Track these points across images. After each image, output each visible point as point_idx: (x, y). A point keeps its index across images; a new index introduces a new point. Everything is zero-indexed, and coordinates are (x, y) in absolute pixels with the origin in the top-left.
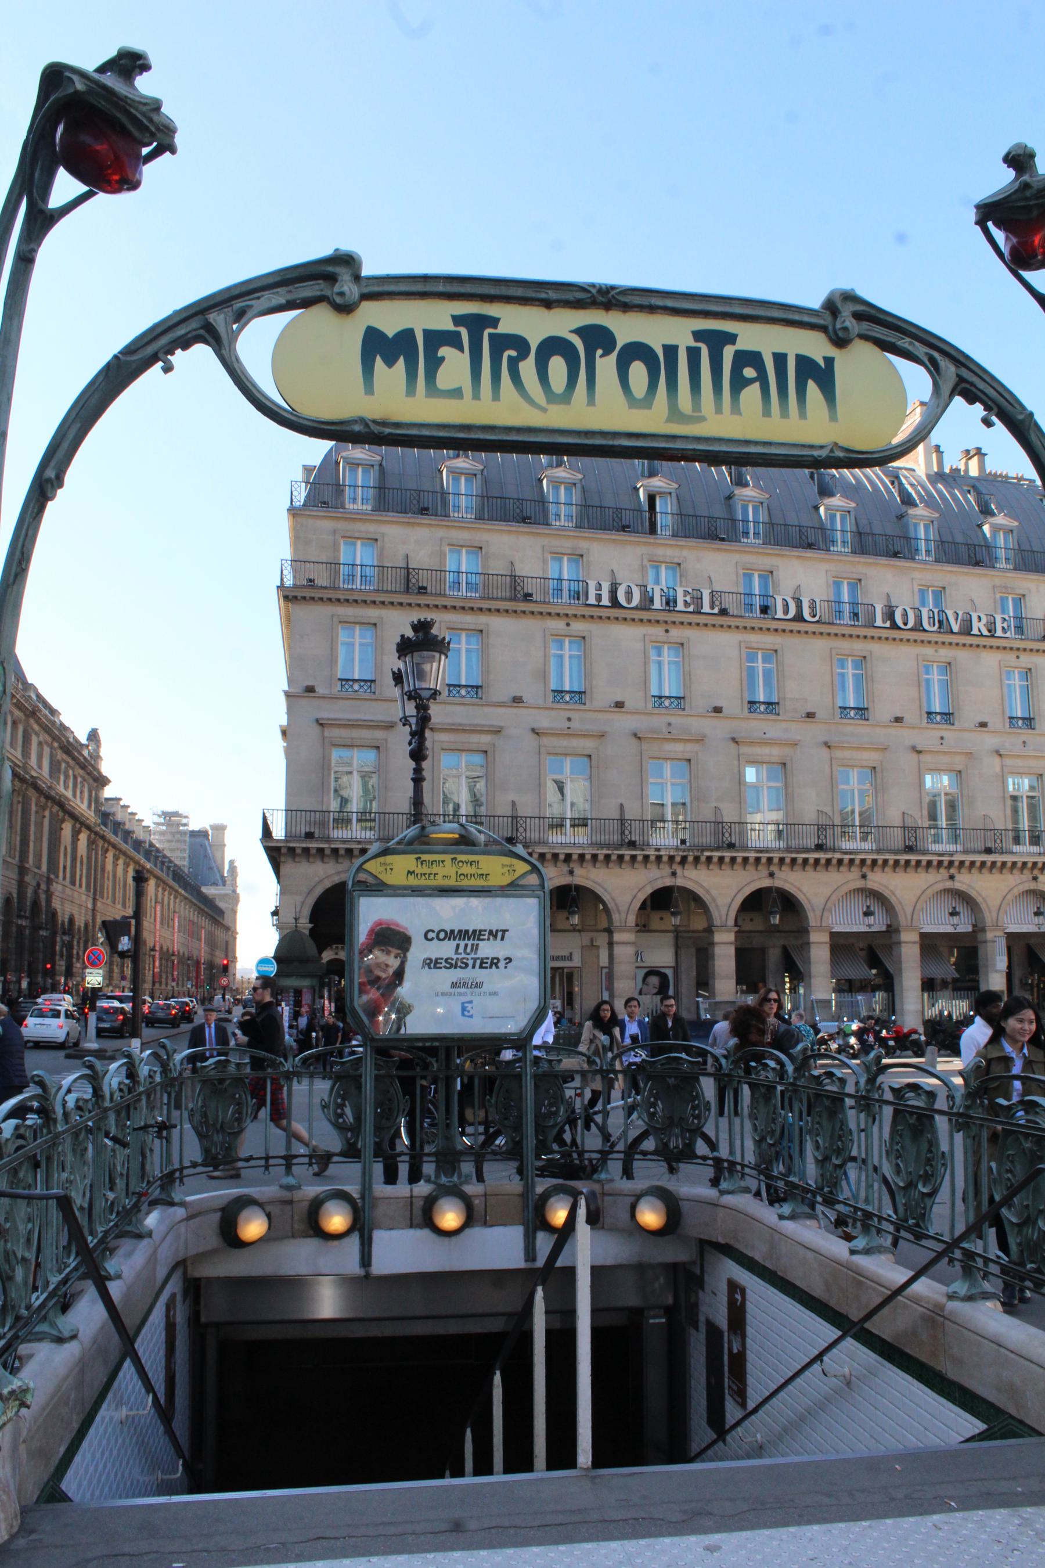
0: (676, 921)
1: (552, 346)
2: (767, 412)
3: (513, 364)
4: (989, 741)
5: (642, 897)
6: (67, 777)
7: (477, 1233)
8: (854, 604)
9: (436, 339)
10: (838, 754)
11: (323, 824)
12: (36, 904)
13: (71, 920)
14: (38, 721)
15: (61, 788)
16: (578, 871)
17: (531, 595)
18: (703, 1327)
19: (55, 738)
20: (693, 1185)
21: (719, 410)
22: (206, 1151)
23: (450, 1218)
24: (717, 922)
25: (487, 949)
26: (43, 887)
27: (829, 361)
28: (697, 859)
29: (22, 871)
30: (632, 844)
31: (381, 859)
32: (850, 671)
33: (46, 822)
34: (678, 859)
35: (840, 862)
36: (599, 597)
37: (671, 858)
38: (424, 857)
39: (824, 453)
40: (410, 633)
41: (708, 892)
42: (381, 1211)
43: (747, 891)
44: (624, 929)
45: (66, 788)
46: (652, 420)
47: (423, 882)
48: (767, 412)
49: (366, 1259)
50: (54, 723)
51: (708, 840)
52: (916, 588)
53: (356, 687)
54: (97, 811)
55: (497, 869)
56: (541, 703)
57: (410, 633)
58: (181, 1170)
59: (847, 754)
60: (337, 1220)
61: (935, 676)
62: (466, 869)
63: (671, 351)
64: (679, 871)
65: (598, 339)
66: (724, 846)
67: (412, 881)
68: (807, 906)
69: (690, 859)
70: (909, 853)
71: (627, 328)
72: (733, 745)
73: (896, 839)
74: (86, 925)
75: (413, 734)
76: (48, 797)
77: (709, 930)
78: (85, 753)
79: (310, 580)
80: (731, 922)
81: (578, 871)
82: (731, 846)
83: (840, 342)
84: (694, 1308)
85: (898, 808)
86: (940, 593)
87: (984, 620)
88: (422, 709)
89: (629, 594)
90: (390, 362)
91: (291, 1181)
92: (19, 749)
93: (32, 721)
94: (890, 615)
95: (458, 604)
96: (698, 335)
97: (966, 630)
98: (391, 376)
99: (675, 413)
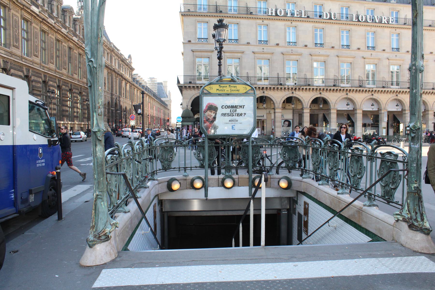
0: (293, 106)
4: (385, 55)
5: (284, 99)
6: (123, 68)
7: (236, 188)
8: (347, 14)
10: (341, 59)
11: (194, 79)
12: (116, 104)
13: (126, 108)
14: (114, 53)
15: (121, 72)
16: (266, 92)
17: (252, 13)
18: (297, 214)
20: (295, 176)
22: (163, 166)
23: (229, 184)
24: (305, 107)
25: (239, 111)
26: (118, 99)
28: (299, 89)
29: (112, 95)
30: (281, 84)
31: (209, 86)
32: (345, 34)
34: (294, 89)
35: (340, 90)
36: (272, 13)
37: (292, 88)
38: (221, 85)
40: (217, 23)
41: (302, 98)
42: (210, 182)
43: (314, 98)
44: (278, 108)
45: (123, 71)
47: (221, 92)
49: (206, 195)
50: (118, 53)
51: (302, 83)
52: (366, 9)
53: (203, 40)
54: (132, 77)
55: (242, 88)
56: (255, 44)
57: (217, 23)
58: (156, 171)
59: (343, 59)
60: (198, 184)
61: (370, 36)
62: (233, 89)
64: (294, 92)
66: (307, 85)
67: (218, 92)
68: (330, 102)
69: (297, 89)
70: (360, 88)
72: (310, 56)
73: (357, 83)
74: (130, 109)
75: (218, 52)
76: (118, 74)
77: (302, 109)
78: (128, 61)
80: (309, 106)
81: (266, 92)
82: (309, 85)
84: (295, 209)
85: (358, 74)
86: (373, 10)
87: (386, 19)
88: (221, 45)
89: (281, 12)
91: (186, 174)
92: (109, 61)
93: (112, 53)
94: (358, 18)
95: (231, 16)
97: (381, 22)
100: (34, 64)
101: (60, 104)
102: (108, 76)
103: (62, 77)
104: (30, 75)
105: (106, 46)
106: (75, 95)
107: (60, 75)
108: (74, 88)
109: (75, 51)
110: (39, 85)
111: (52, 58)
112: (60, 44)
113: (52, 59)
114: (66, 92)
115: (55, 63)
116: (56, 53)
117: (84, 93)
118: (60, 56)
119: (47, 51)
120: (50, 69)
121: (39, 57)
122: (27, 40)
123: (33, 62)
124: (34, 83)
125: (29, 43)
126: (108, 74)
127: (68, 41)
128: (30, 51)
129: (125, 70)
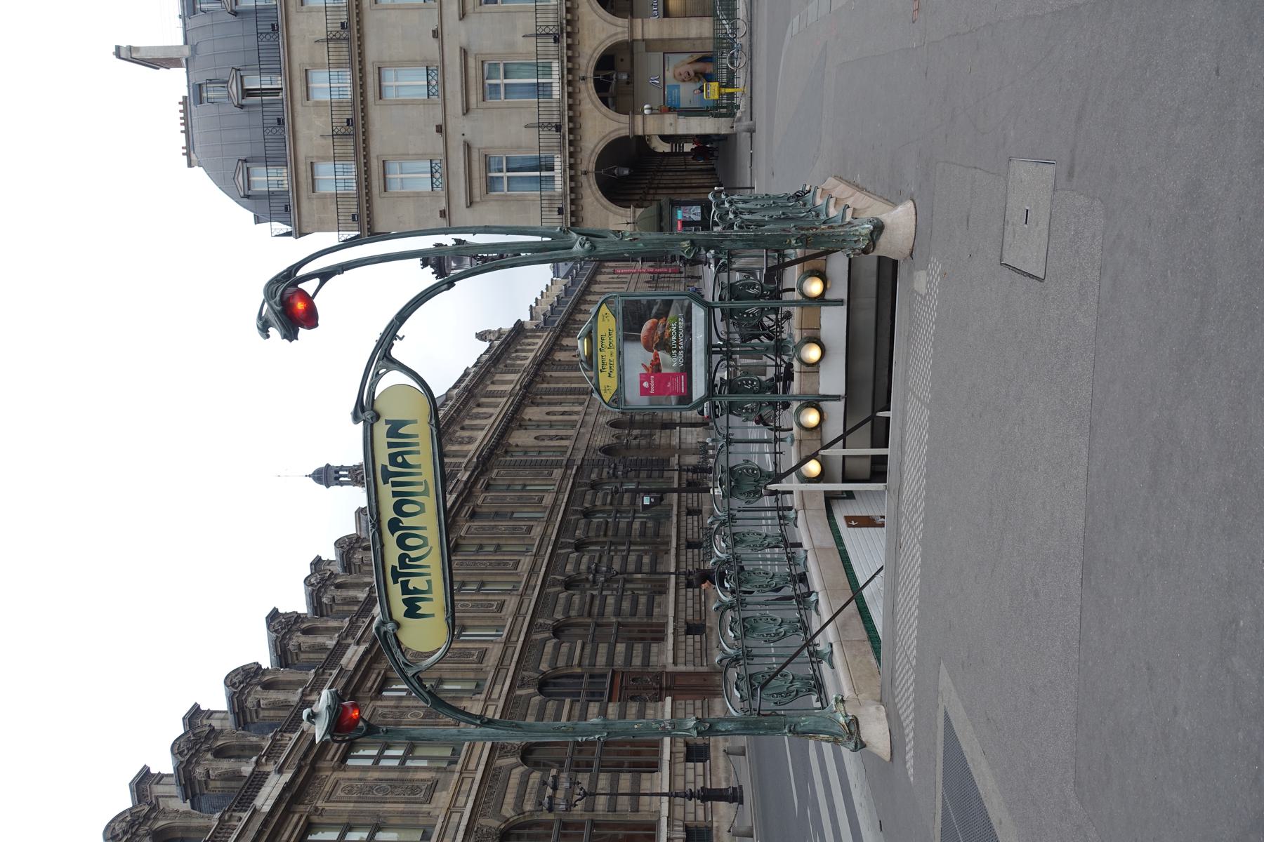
1: (401, 542)
2: (418, 452)
6: (518, 358)
7: (824, 334)
9: (405, 589)
11: (551, 199)
17: (342, 24)
19: (488, 371)
21: (420, 474)
23: (813, 353)
27: (387, 422)
33: (555, 374)
45: (526, 358)
46: (430, 502)
47: (615, 368)
48: (418, 452)
50: (476, 373)
54: (542, 330)
60: (812, 418)
62: (606, 343)
63: (395, 494)
65: (394, 525)
67: (615, 374)
71: (388, 513)
76: (536, 375)
78: (497, 343)
79: (353, 216)
83: (377, 416)
90: (419, 608)
91: (789, 440)
92: (499, 400)
95: (359, 91)
96: (386, 482)
98: (424, 607)
99: (426, 493)
100: (523, 610)
101: (624, 544)
102: (543, 404)
104: (550, 622)
105: (458, 411)
106: (598, 503)
107: (545, 542)
109: (479, 502)
110: (576, 599)
111: (501, 564)
114: (593, 526)
115: (516, 558)
116: (489, 553)
117: (594, 476)
118: (495, 542)
119: (485, 578)
120: (532, 571)
121: (502, 598)
123: (517, 614)
124: (573, 613)
126: (538, 405)
128: (489, 623)
129: (523, 351)
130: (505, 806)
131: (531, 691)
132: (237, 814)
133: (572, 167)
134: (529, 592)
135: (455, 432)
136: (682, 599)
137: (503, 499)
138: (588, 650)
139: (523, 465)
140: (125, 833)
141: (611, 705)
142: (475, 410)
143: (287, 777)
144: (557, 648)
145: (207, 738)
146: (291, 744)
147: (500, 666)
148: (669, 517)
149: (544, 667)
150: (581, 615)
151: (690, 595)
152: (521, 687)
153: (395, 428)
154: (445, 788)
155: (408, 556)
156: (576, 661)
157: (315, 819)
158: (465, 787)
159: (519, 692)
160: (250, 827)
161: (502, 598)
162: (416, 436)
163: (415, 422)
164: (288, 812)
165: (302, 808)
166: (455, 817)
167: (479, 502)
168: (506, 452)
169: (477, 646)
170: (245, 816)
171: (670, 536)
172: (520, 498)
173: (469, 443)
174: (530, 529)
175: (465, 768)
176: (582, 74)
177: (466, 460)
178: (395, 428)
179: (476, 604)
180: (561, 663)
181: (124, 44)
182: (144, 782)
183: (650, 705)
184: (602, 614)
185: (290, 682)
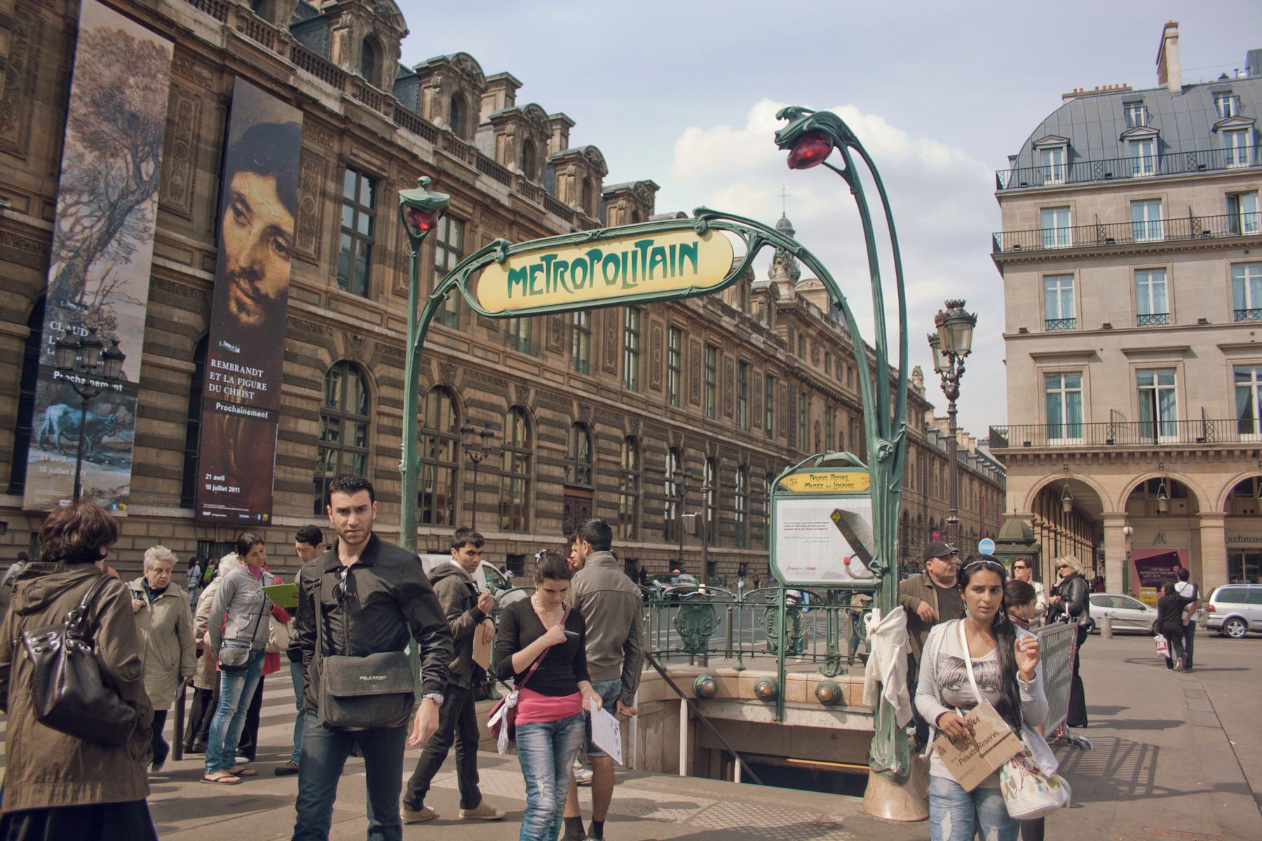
1: (579, 262)
2: (665, 276)
3: (562, 273)
22: (687, 645)
27: (695, 244)
39: (686, 292)
40: (945, 310)
46: (615, 291)
48: (665, 276)
56: (1225, 321)
62: (840, 481)
63: (625, 255)
65: (595, 255)
67: (808, 489)
71: (606, 249)
74: (919, 517)
83: (703, 233)
92: (855, 388)
96: (637, 245)
98: (518, 288)
99: (625, 285)
100: (651, 409)
103: (721, 437)
106: (754, 480)
108: (751, 464)
109: (756, 369)
112: (717, 355)
113: (696, 393)
119: (682, 374)
120: (688, 418)
121: (664, 390)
122: (636, 354)
123: (648, 404)
124: (648, 455)
125: (641, 359)
127: (739, 345)
128: (641, 377)
130: (472, 391)
131: (576, 415)
132: (475, 161)
133: (1072, 456)
134: (669, 414)
135: (824, 347)
136: (660, 556)
137: (759, 391)
138: (613, 467)
139: (792, 409)
140: (463, 70)
141: (561, 487)
142: (844, 365)
143: (506, 202)
144: (616, 439)
145: (542, 133)
146: (534, 204)
147: (599, 388)
148: (737, 546)
149: (598, 427)
150: (646, 462)
151: (663, 563)
152: (580, 405)
153: (689, 251)
154: (490, 337)
155: (566, 270)
156: (603, 457)
157: (468, 226)
158: (491, 356)
159: (575, 404)
160: (464, 172)
161: (664, 390)
162: (681, 274)
163: (695, 272)
164: (475, 203)
165: (478, 214)
166: (464, 347)
167: (756, 369)
168: (804, 394)
169: (619, 366)
170: (473, 168)
171: (720, 546)
172: (759, 406)
173: (813, 359)
174: (730, 415)
175: (508, 356)
176: (1166, 466)
177: (796, 357)
178: (689, 251)
179: (658, 366)
180: (602, 443)
181: (1180, 30)
182: (510, 84)
183: (560, 524)
184: (647, 481)
185: (590, 202)
